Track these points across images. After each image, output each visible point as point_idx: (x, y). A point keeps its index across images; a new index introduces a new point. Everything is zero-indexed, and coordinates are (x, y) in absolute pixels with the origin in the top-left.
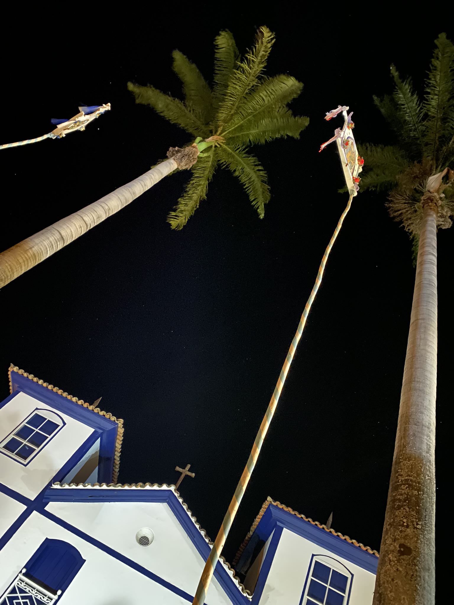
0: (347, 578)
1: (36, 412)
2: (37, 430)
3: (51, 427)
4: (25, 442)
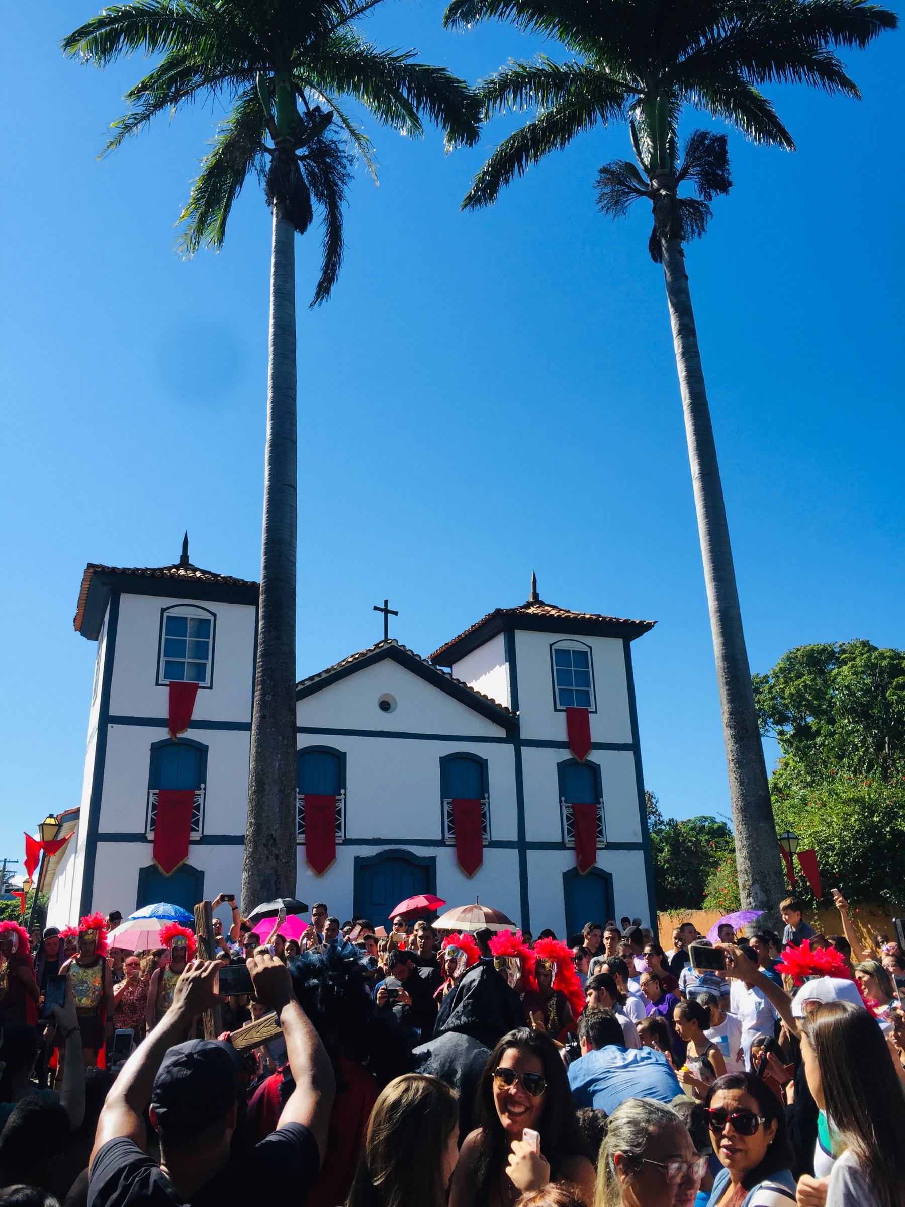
0: (586, 652)
1: (165, 614)
2: (187, 639)
3: (204, 627)
4: (186, 660)
